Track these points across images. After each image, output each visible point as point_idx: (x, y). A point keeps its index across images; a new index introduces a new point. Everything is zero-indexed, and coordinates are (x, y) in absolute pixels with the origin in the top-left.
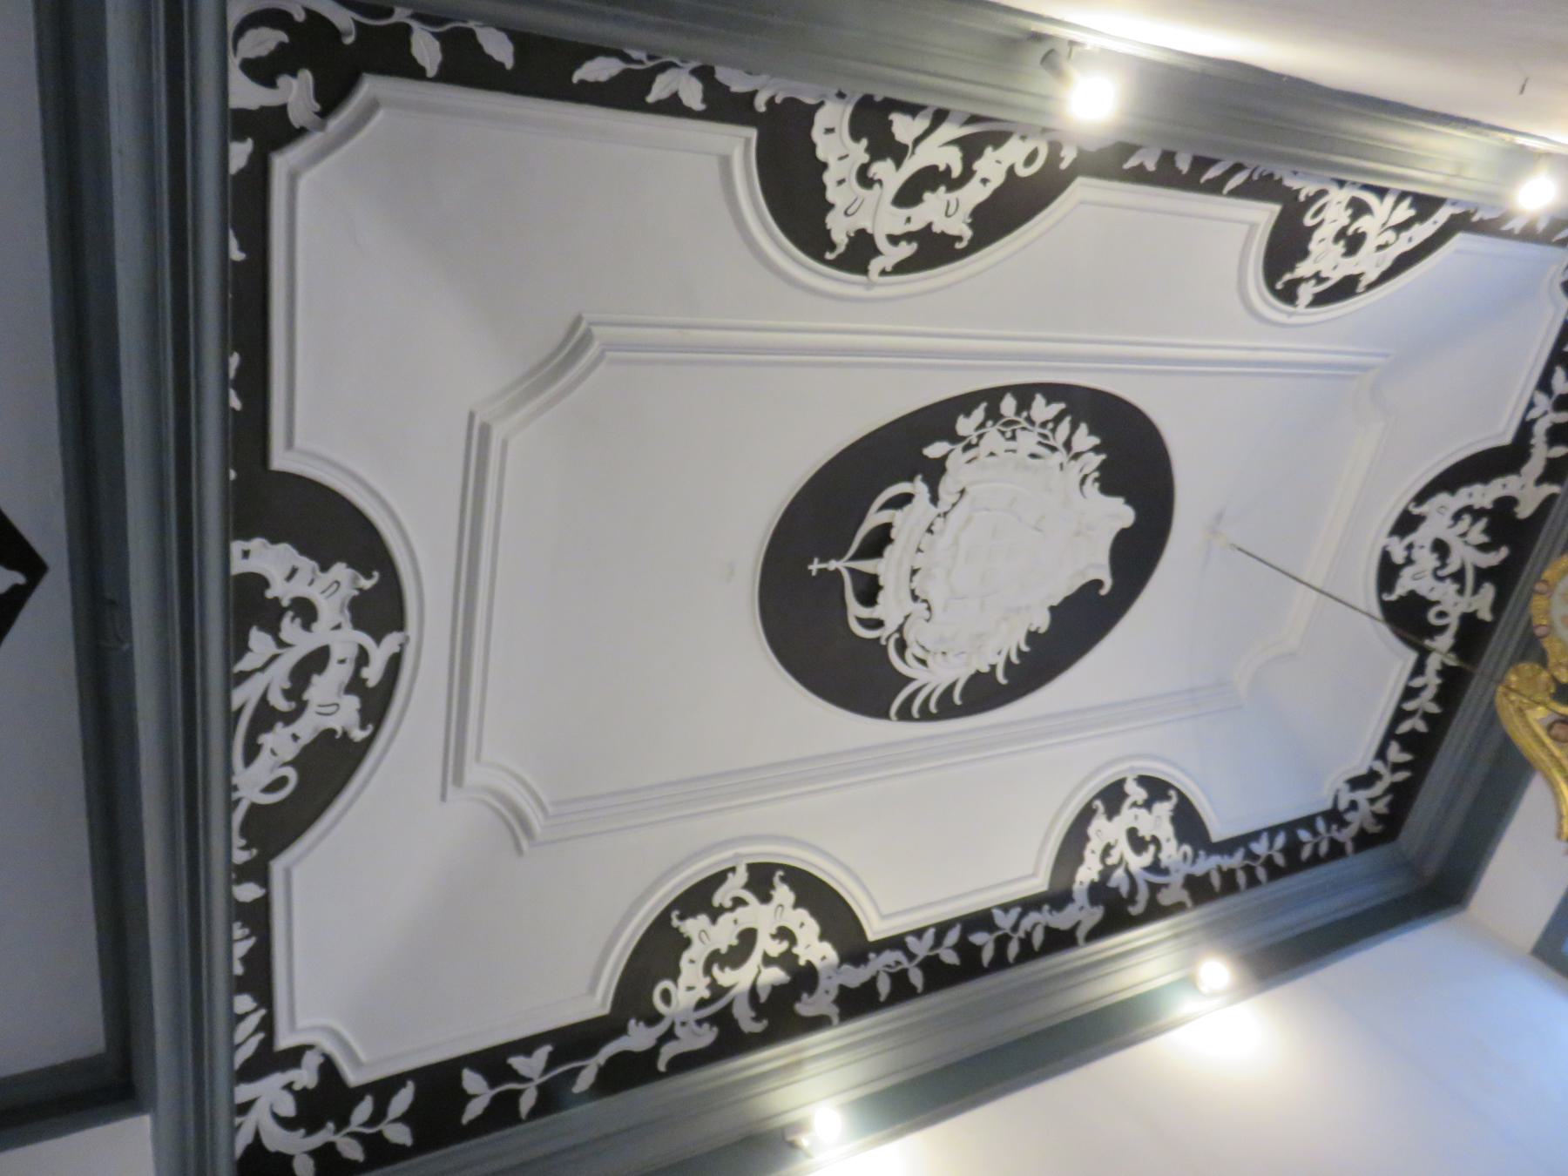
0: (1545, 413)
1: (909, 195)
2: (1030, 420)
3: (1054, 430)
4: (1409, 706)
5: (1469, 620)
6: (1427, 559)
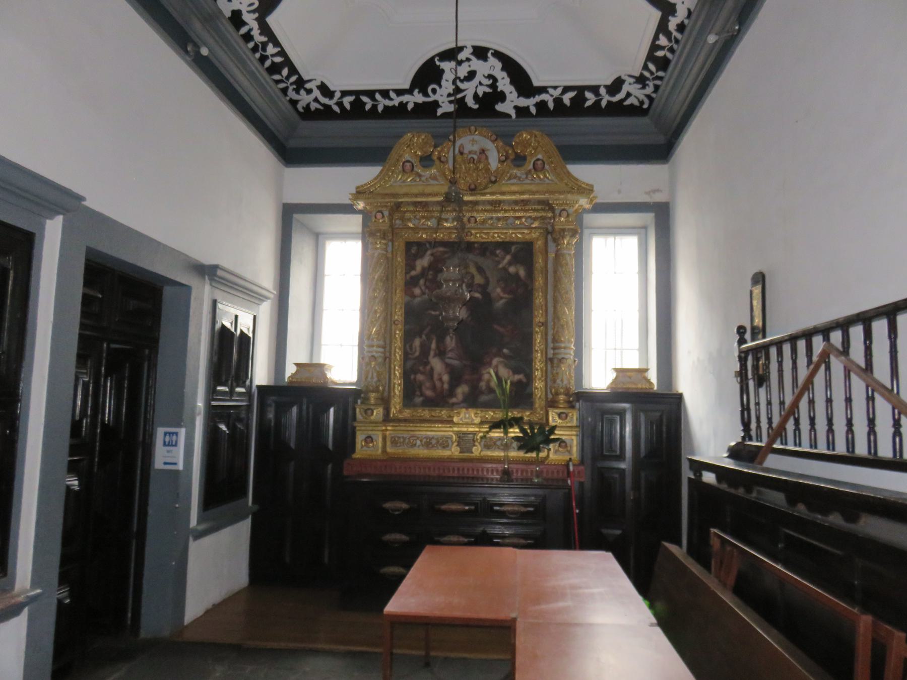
0: (552, 96)
4: (378, 96)
5: (436, 104)
6: (463, 71)
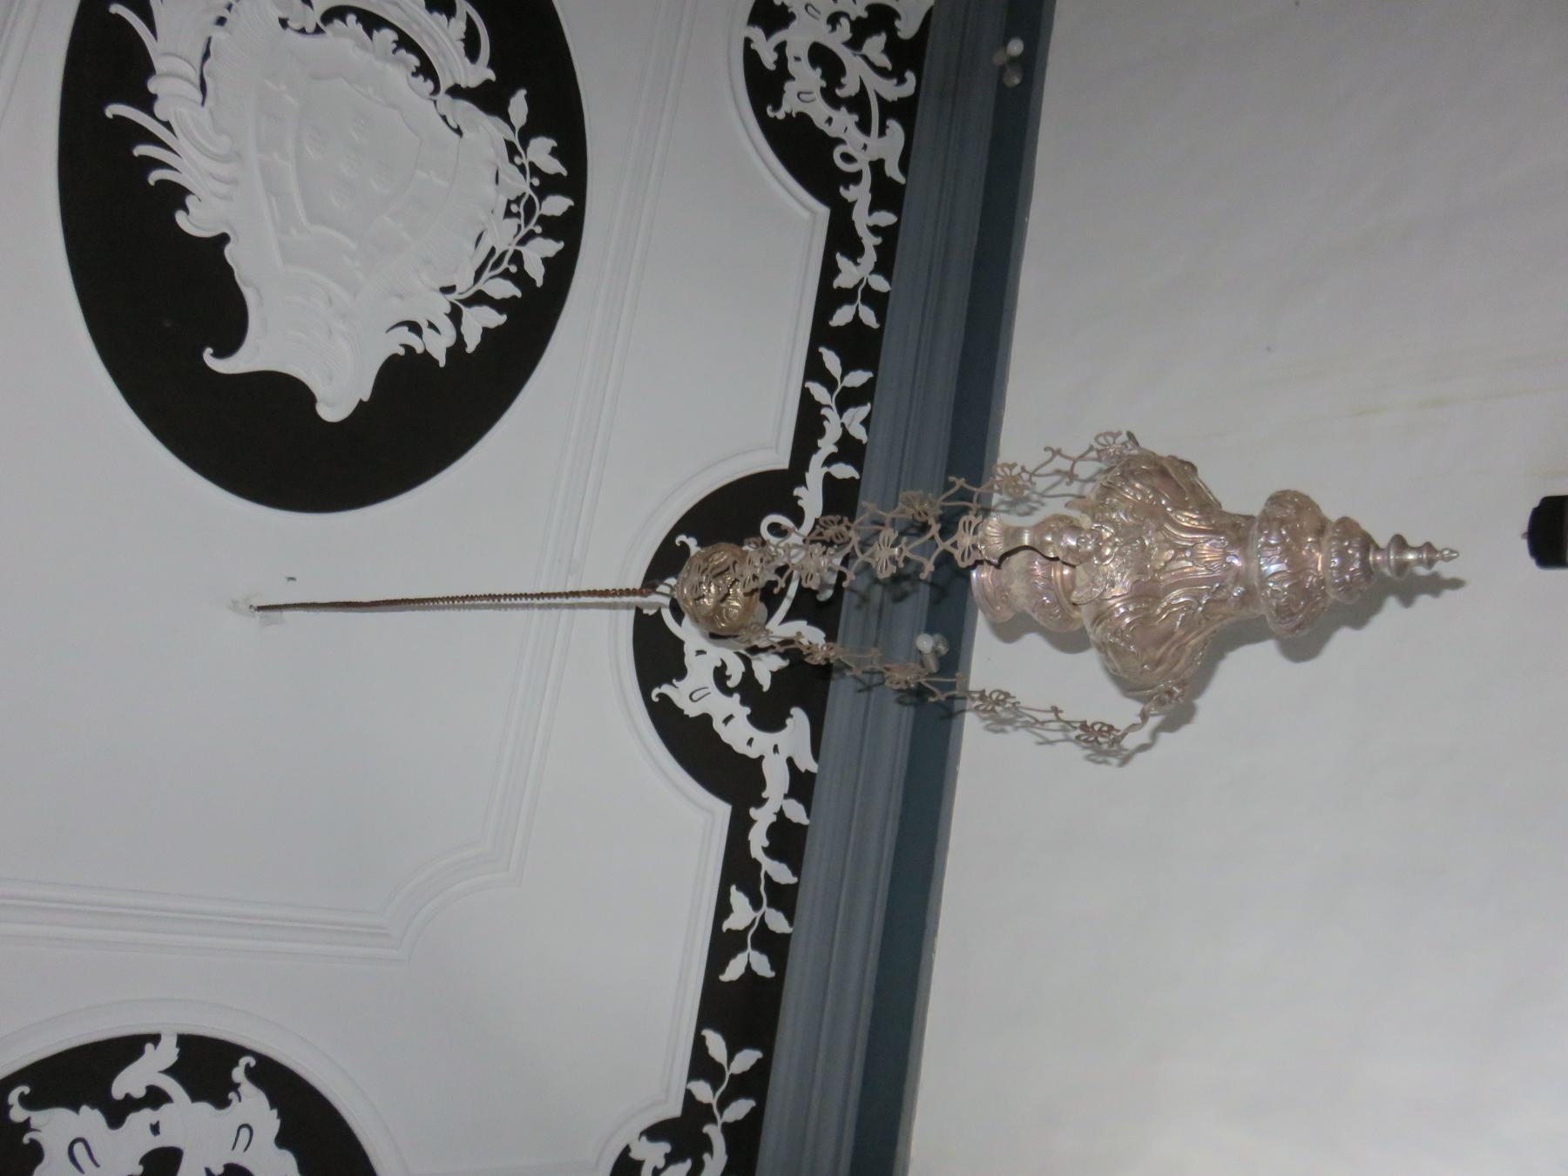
1: (820, 56)
2: (531, 235)
3: (506, 275)
